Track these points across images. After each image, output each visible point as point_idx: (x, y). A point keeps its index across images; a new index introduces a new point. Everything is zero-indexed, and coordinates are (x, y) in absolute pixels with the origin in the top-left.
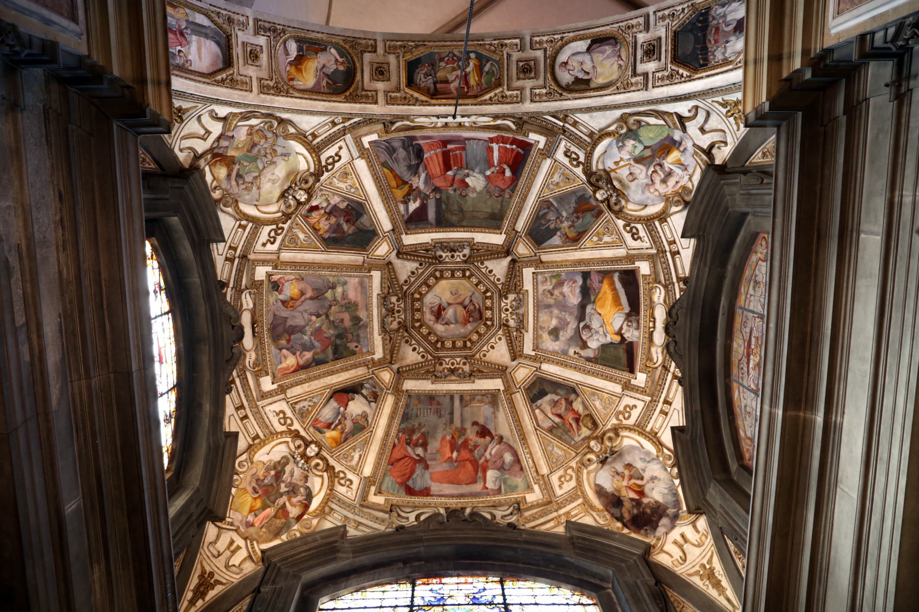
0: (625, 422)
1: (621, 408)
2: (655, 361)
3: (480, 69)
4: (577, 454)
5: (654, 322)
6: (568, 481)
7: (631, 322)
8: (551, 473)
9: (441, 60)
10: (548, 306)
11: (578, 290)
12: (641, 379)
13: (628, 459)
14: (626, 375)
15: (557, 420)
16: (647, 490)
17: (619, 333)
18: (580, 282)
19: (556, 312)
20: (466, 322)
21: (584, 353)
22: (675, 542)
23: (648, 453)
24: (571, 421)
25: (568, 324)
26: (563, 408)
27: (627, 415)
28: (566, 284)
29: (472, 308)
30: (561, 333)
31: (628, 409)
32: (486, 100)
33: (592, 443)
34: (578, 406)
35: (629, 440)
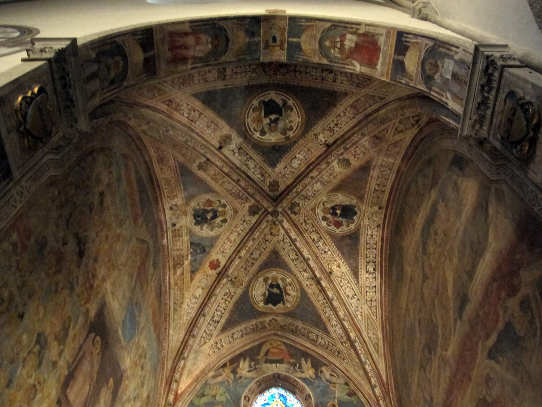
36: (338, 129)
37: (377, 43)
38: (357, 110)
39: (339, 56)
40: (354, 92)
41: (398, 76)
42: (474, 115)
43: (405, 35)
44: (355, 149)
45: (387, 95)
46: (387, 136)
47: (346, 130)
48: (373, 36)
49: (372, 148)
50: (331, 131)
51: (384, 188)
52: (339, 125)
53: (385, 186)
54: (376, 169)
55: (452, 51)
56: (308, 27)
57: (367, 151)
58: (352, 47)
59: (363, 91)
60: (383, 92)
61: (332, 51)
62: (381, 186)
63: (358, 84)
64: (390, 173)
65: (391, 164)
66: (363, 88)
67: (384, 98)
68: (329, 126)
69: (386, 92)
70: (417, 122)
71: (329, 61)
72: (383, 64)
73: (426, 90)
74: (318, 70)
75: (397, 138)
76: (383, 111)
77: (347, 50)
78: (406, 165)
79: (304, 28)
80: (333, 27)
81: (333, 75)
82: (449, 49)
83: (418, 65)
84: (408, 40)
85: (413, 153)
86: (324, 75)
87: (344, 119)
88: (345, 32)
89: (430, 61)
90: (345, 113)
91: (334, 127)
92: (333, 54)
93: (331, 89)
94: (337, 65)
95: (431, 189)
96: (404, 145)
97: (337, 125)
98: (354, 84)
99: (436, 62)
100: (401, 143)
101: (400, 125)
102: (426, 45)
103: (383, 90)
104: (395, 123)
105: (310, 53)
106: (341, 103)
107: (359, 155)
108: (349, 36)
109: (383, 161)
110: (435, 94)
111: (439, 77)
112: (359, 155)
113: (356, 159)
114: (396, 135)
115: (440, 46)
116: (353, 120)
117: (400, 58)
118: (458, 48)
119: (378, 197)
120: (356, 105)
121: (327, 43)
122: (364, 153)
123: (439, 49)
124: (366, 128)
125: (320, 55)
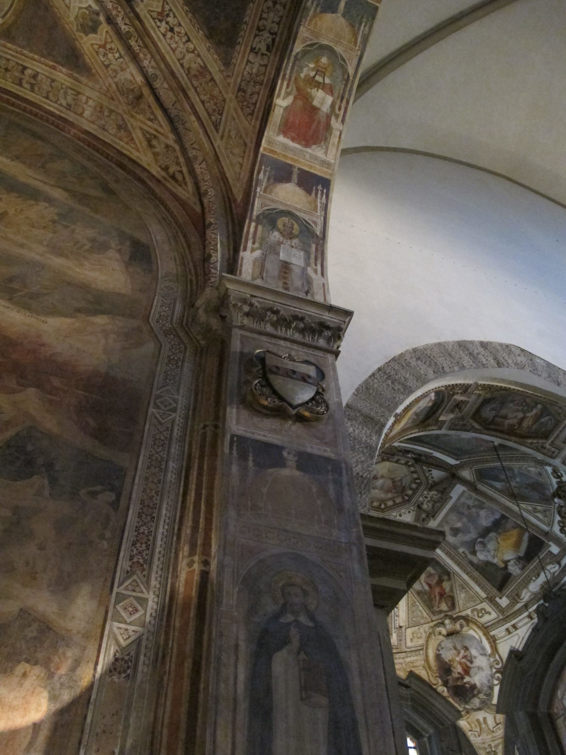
0: (476, 618)
1: (479, 607)
2: (522, 597)
3: (537, 418)
4: (432, 621)
5: (537, 578)
6: (418, 638)
7: (519, 563)
8: (409, 627)
9: (512, 401)
10: (462, 514)
11: (492, 519)
12: (504, 602)
13: (467, 643)
14: (495, 591)
15: (427, 588)
16: (472, 672)
17: (506, 563)
18: (497, 516)
19: (465, 520)
20: (388, 491)
21: (470, 557)
22: (478, 721)
23: (483, 648)
24: (437, 594)
25: (470, 532)
26: (435, 581)
27: (480, 615)
28: (485, 510)
29: (399, 484)
30: (460, 535)
31: (483, 612)
32: (526, 443)
33: (447, 621)
34: (446, 585)
35: (473, 632)
36: (163, 30)
37: (315, 143)
38: (195, 76)
39: (302, 75)
40: (229, 80)
41: (268, 169)
42: (258, 302)
43: (325, 191)
44: (118, 50)
45: (222, 137)
46: (140, 117)
47: (159, 44)
48: (326, 139)
49: (116, 84)
50: (159, 14)
51: (27, 86)
52: (169, 34)
53: (32, 90)
54: (71, 80)
55: (316, 265)
56: (355, 35)
57: (111, 72)
58: (313, 99)
59: (230, 96)
60: (230, 131)
61: (312, 65)
62: (33, 81)
63: (244, 92)
64: (61, 105)
65: (80, 111)
66: (237, 97)
67: (217, 131)
68: (171, 15)
69: (229, 137)
70: (173, 177)
71: (297, 54)
72: (285, 147)
73: (255, 213)
74: (277, 26)
75: (138, 135)
76: (196, 124)
77: (309, 90)
78: (79, 139)
79: (356, 28)
80: (346, 77)
81: (264, 50)
82: (316, 259)
83: (286, 205)
84: (319, 196)
85: (107, 156)
86: (266, 34)
87: (181, 48)
88: (336, 95)
89: (296, 226)
90: (193, 52)
91: (167, 23)
92: (307, 66)
93: (240, 40)
94: (290, 68)
95: (66, 190)
96: (122, 143)
97: (172, 30)
98: (243, 84)
99: (296, 237)
100: (126, 140)
101: (163, 146)
102: (315, 223)
103: (233, 134)
104: (167, 137)
105: (316, 24)
106: (212, 51)
107: (105, 55)
108: (329, 100)
109: (87, 97)
110: (252, 229)
111: (276, 239)
112: (105, 55)
113: (96, 47)
114: (144, 135)
115: (317, 245)
116: (179, 65)
117: (295, 177)
118: (323, 274)
119: (7, 70)
120: (205, 77)
121: (324, 60)
122: (107, 67)
123: (314, 243)
124: (166, 86)
125: (309, 43)
